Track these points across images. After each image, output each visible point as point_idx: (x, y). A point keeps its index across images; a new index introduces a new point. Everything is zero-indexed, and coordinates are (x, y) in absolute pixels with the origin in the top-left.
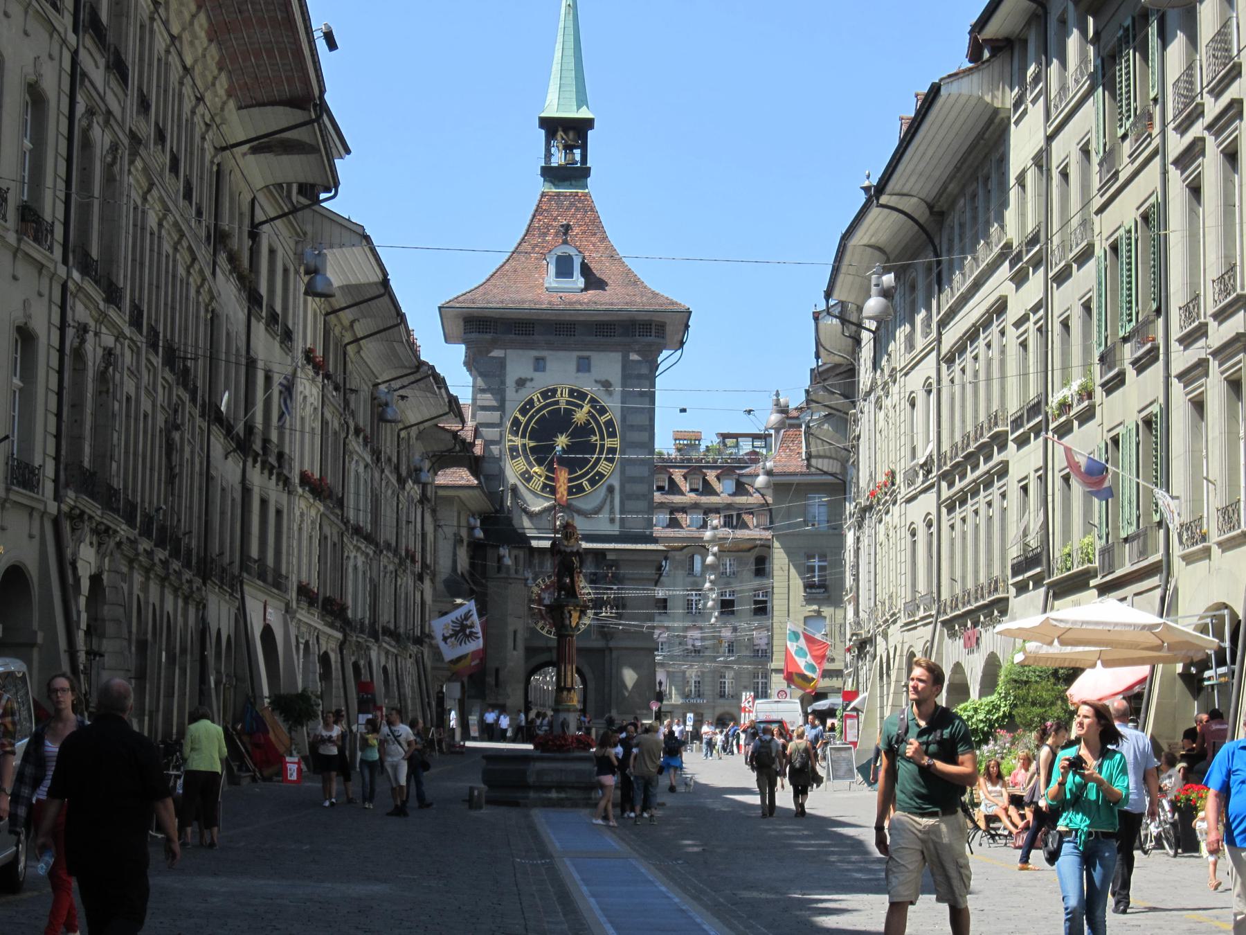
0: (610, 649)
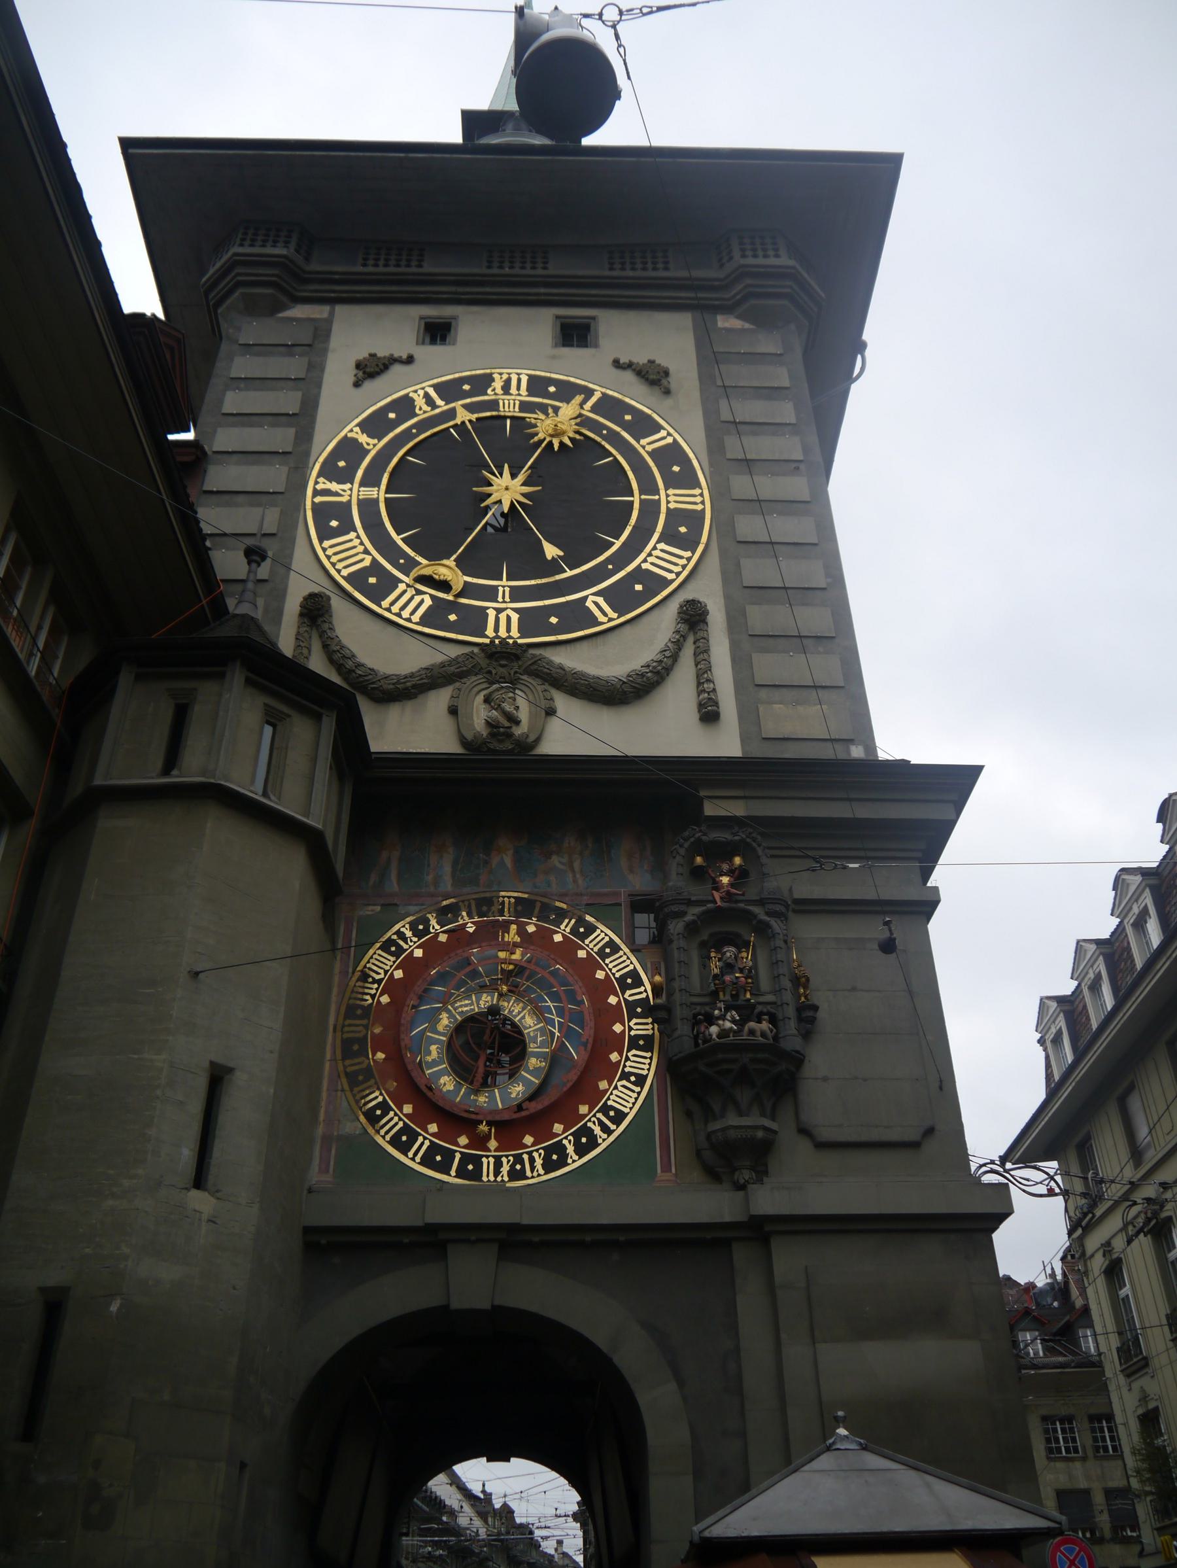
0: (761, 1231)
